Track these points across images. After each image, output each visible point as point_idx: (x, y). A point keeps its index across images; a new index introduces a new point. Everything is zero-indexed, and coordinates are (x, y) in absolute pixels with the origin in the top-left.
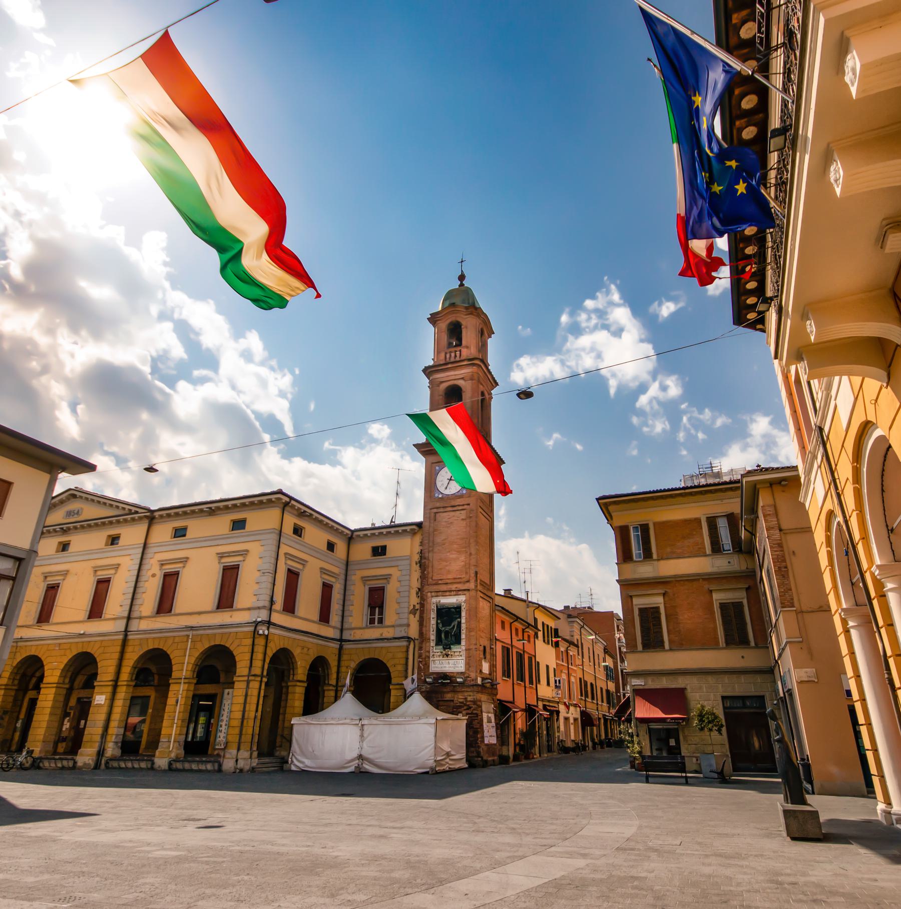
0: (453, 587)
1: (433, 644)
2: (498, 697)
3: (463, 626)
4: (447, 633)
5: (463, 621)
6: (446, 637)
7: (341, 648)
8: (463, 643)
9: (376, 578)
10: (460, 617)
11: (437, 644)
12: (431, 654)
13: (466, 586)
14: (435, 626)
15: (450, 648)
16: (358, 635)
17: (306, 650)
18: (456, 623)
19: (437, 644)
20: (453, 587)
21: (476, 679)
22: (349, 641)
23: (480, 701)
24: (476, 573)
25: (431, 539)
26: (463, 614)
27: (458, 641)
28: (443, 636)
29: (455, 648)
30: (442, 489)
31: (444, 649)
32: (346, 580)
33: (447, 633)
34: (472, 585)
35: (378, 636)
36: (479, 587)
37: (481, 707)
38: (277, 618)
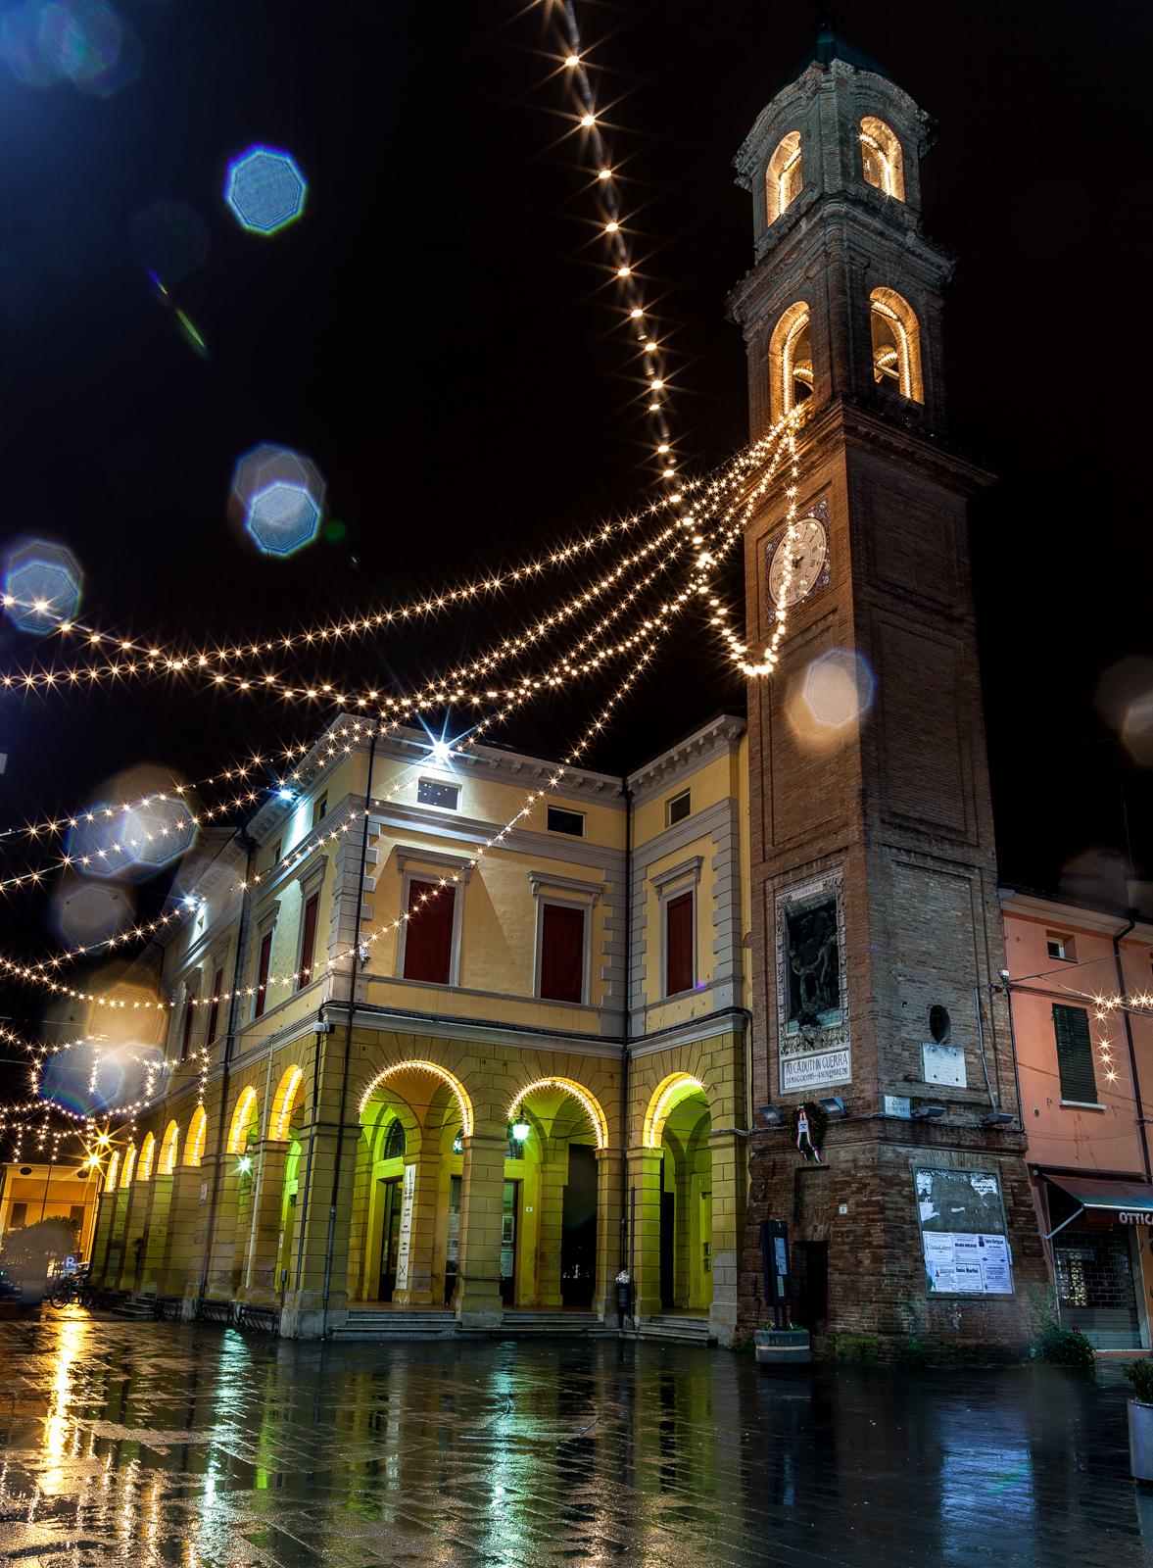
0: (813, 851)
1: (781, 1017)
2: (1034, 1156)
3: (842, 953)
4: (810, 981)
5: (842, 939)
6: (810, 992)
7: (626, 1060)
8: (845, 1001)
9: (674, 875)
11: (791, 1018)
12: (782, 1044)
13: (839, 841)
14: (781, 968)
15: (816, 1023)
16: (656, 1020)
18: (823, 950)
19: (791, 1018)
20: (813, 851)
22: (640, 1039)
23: (906, 1166)
24: (864, 794)
25: (766, 738)
26: (841, 920)
27: (833, 1003)
28: (802, 988)
29: (832, 1020)
31: (802, 1024)
32: (628, 896)
33: (810, 981)
34: (853, 833)
35: (685, 1018)
36: (877, 834)
38: (374, 995)
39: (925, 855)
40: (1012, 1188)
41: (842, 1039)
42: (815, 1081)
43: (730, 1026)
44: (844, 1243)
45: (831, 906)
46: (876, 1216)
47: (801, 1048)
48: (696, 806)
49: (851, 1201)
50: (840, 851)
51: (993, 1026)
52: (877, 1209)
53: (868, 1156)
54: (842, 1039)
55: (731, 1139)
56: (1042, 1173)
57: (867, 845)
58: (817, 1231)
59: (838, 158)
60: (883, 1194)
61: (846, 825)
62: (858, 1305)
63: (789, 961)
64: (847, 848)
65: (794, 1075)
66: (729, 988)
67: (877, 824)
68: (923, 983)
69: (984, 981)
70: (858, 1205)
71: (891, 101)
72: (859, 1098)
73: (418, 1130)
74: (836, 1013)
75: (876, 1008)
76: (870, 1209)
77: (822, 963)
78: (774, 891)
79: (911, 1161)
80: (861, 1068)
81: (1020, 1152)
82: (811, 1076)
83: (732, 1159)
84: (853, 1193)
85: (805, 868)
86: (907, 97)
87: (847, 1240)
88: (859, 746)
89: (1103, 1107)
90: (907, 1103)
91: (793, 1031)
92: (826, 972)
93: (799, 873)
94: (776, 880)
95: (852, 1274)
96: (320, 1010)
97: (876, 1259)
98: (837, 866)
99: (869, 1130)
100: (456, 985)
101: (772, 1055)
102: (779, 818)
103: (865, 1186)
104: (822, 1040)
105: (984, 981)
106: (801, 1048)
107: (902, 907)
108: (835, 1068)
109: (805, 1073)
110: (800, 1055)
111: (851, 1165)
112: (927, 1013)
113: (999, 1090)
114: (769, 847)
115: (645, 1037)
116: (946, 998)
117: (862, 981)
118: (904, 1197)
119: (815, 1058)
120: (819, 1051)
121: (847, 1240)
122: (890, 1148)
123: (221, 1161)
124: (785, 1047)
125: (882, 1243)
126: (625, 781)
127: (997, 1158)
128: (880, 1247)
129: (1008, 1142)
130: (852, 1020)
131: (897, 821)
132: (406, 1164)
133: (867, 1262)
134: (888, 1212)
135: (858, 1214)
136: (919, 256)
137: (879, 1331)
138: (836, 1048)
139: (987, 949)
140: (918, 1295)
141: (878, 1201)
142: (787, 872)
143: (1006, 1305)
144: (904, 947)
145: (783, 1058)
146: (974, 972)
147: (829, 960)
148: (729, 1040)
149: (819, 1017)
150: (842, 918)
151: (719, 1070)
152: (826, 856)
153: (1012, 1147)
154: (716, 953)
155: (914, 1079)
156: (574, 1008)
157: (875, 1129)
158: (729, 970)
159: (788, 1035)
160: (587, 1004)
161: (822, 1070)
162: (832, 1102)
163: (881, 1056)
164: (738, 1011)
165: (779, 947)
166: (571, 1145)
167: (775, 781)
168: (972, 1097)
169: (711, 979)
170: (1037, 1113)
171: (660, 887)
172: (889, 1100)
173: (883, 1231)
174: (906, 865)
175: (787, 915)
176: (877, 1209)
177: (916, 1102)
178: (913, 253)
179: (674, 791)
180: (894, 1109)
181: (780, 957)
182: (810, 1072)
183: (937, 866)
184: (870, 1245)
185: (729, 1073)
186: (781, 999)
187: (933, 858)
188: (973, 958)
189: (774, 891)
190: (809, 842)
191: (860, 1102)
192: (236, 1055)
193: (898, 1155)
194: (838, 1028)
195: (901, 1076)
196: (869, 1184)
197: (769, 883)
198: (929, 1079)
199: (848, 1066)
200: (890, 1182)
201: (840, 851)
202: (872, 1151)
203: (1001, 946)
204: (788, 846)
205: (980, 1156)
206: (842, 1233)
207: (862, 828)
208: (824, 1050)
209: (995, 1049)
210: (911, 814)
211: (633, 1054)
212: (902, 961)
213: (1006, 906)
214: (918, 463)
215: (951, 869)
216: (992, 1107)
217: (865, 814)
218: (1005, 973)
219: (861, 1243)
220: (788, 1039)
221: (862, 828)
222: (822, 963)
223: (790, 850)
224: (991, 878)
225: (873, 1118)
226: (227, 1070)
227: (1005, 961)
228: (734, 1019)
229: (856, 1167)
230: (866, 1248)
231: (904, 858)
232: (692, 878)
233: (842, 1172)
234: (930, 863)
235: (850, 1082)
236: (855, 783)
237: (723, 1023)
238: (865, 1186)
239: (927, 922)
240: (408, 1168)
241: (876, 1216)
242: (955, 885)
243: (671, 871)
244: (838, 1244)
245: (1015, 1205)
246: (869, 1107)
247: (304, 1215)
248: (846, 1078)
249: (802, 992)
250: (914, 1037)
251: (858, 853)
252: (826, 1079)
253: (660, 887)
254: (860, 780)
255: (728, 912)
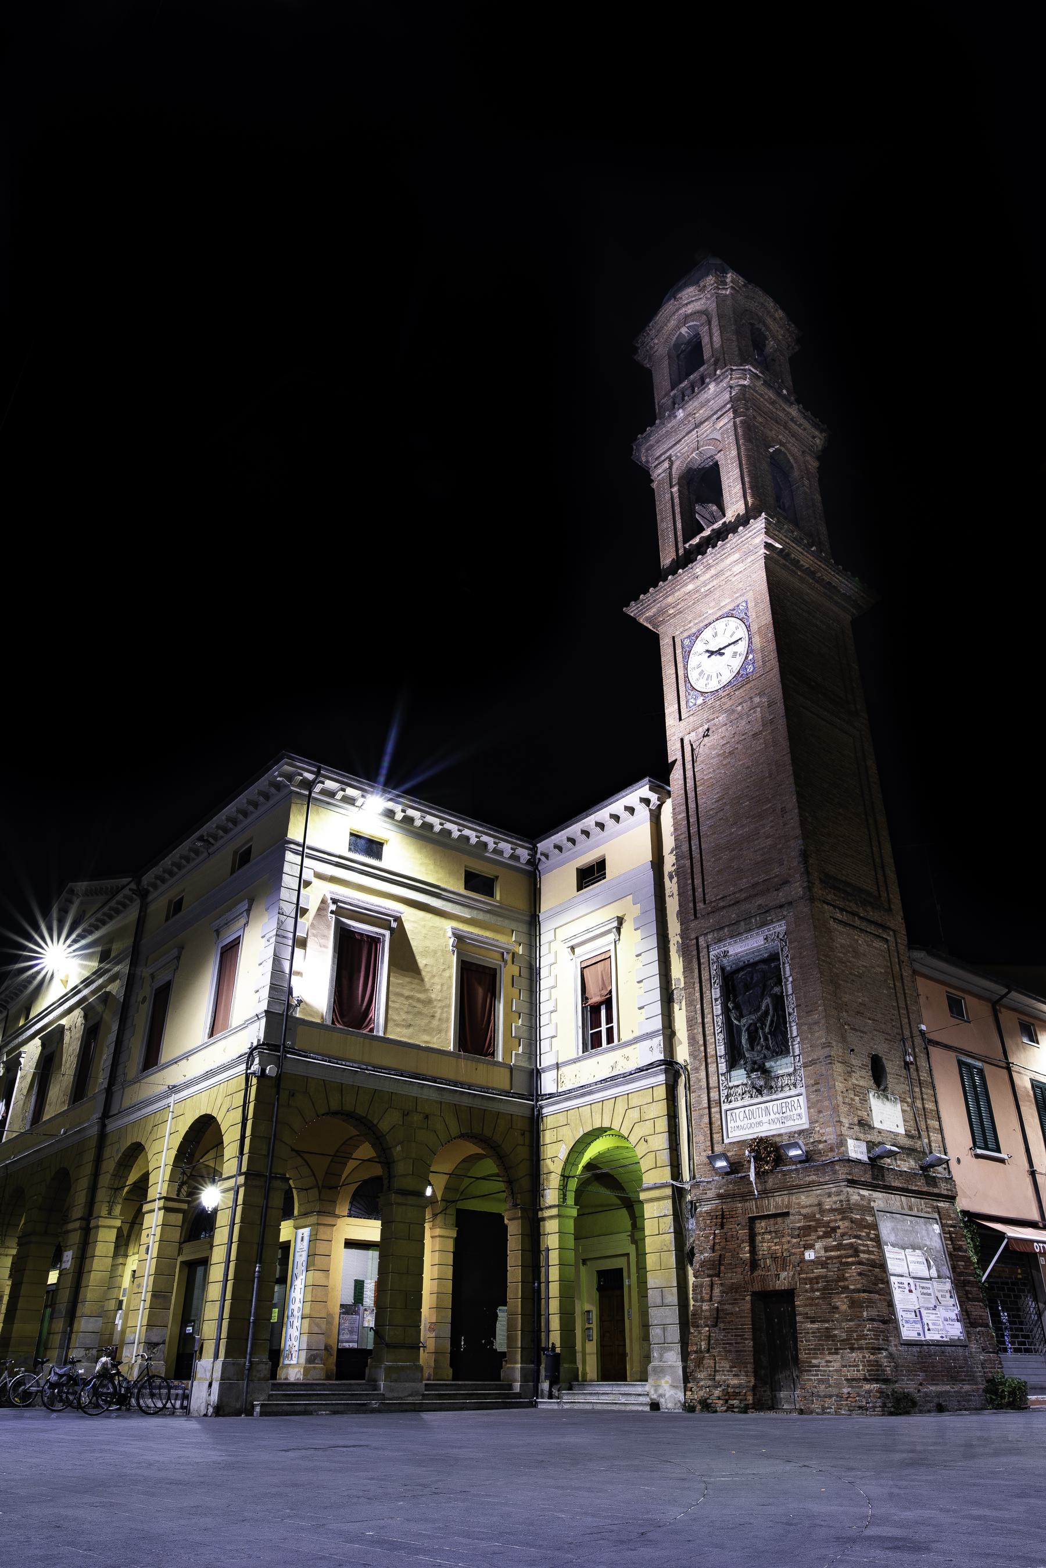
1: (723, 1068)
2: (963, 1203)
6: (753, 1040)
10: (779, 982)
11: (732, 1065)
13: (781, 896)
14: (719, 1020)
17: (416, 1118)
19: (732, 1065)
21: (842, 1143)
22: (551, 1095)
23: (870, 1210)
24: (805, 855)
30: (700, 686)
34: (797, 889)
36: (817, 890)
37: (875, 1226)
39: (854, 914)
40: (950, 1233)
41: (795, 1085)
42: (766, 1127)
43: (662, 1078)
44: (813, 1290)
45: (774, 957)
46: (850, 1260)
47: (747, 1095)
48: (611, 870)
49: (818, 1245)
50: (781, 906)
51: (919, 1076)
52: (850, 1252)
53: (835, 1198)
54: (795, 1085)
55: (668, 1191)
56: (972, 1218)
57: (812, 900)
58: (784, 1280)
59: (735, 343)
60: (856, 1237)
61: (786, 882)
62: (837, 1354)
63: (726, 1011)
64: (790, 903)
65: (739, 1123)
66: (659, 1040)
67: (817, 882)
68: (862, 1032)
69: (907, 1033)
70: (827, 1249)
71: (769, 312)
72: (820, 1142)
73: (316, 1191)
74: (785, 1061)
75: (832, 1053)
76: (843, 1252)
77: (766, 1013)
78: (708, 947)
79: (872, 1204)
80: (820, 1112)
81: (952, 1198)
82: (759, 1123)
83: (669, 1210)
84: (819, 1237)
85: (742, 923)
86: (780, 312)
87: (816, 1286)
88: (796, 811)
89: (1006, 1157)
90: (863, 1147)
91: (739, 1076)
92: (772, 1022)
93: (736, 929)
94: (710, 936)
95: (827, 1321)
96: (251, 1053)
97: (853, 1304)
98: (779, 921)
99: (835, 1172)
100: (381, 1034)
101: (713, 1104)
102: (709, 880)
103: (834, 1230)
104: (772, 1087)
105: (907, 1033)
106: (747, 1095)
107: (841, 962)
108: (788, 1114)
109: (753, 1120)
110: (746, 1103)
111: (816, 1209)
112: (868, 1061)
113: (929, 1138)
114: (700, 906)
115: (559, 1094)
116: (881, 1048)
117: (816, 1028)
118: (871, 1240)
119: (763, 1106)
120: (768, 1098)
121: (816, 1286)
122: (856, 1190)
123: (92, 1225)
124: (727, 1097)
125: (859, 1286)
126: (534, 850)
127: (935, 1204)
128: (858, 1291)
129: (943, 1188)
130: (805, 1065)
131: (830, 882)
132: (297, 1228)
133: (844, 1307)
134: (862, 1255)
135: (828, 1258)
136: (800, 425)
137: (865, 1379)
138: (788, 1094)
139: (906, 1004)
140: (893, 1341)
141: (851, 1243)
142: (722, 928)
143: (961, 1350)
144: (846, 998)
145: (725, 1107)
146: (898, 1025)
147: (775, 1009)
148: (661, 1092)
149: (767, 1065)
150: (788, 969)
151: (650, 1123)
152: (766, 912)
153: (945, 1192)
154: (640, 1008)
155: (864, 1125)
156: (489, 1063)
157: (842, 1172)
158: (657, 1024)
159: (731, 1084)
160: (500, 1060)
161: (773, 1116)
162: (795, 1145)
163: (840, 1099)
164: (670, 1066)
165: (716, 1000)
166: (459, 1211)
167: (703, 847)
168: (907, 1142)
169: (637, 1034)
170: (959, 1161)
171: (573, 948)
172: (851, 1143)
173: (860, 1274)
174: (841, 922)
175: (723, 969)
176: (850, 1252)
177: (871, 1145)
178: (795, 423)
179: (587, 858)
180: (856, 1152)
181: (718, 1009)
182: (758, 1120)
183: (864, 925)
184: (845, 1289)
185: (663, 1125)
186: (721, 1050)
187: (860, 917)
188: (896, 1012)
189: (708, 947)
190: (746, 899)
191: (821, 1146)
192: (114, 1111)
193: (863, 1197)
194: (789, 1075)
195: (856, 1120)
196: (839, 1227)
197: (701, 940)
198: (877, 1125)
199: (803, 1111)
200: (861, 1224)
201: (781, 906)
202: (838, 1194)
203: (917, 1002)
204: (722, 904)
205: (923, 1201)
206: (811, 1279)
207: (805, 884)
208: (774, 1097)
209: (923, 1099)
210: (839, 877)
211: (545, 1111)
212: (847, 1012)
213: (917, 966)
214: (817, 582)
215: (872, 929)
216: (924, 1153)
217: (808, 873)
218: (923, 1027)
219: (831, 1287)
220: (730, 1088)
221: (805, 884)
222: (766, 1013)
223: (724, 907)
224: (903, 939)
225: (840, 1160)
226: (103, 1126)
227: (920, 1016)
228: (666, 1071)
229: (822, 1211)
230: (842, 1293)
231: (839, 916)
232: (612, 937)
233: (805, 1216)
234: (857, 922)
235: (806, 1126)
236: (796, 845)
237: (655, 1074)
238: (834, 1230)
239: (860, 976)
240: (301, 1231)
241: (850, 1260)
242: (877, 944)
243: (588, 931)
244: (806, 1291)
245: (955, 1249)
246: (832, 1150)
247: (226, 1275)
248: (803, 1123)
249: (743, 1041)
250: (862, 1083)
251: (804, 909)
252: (778, 1126)
253: (573, 948)
254: (800, 842)
255: (655, 969)
